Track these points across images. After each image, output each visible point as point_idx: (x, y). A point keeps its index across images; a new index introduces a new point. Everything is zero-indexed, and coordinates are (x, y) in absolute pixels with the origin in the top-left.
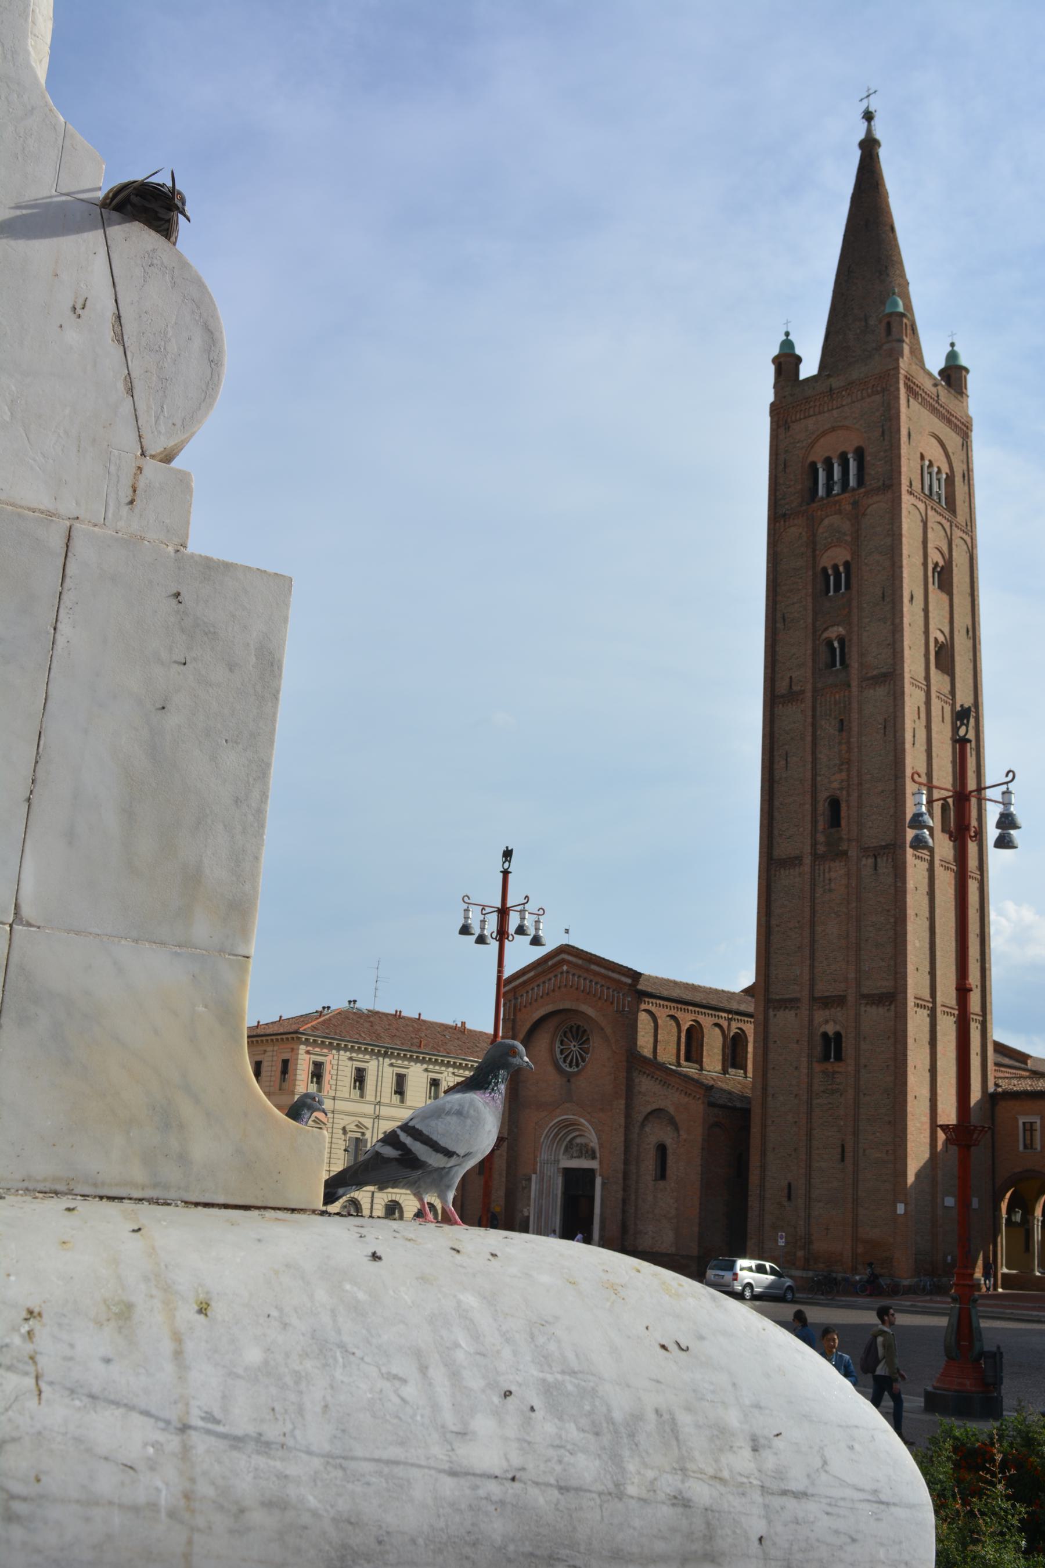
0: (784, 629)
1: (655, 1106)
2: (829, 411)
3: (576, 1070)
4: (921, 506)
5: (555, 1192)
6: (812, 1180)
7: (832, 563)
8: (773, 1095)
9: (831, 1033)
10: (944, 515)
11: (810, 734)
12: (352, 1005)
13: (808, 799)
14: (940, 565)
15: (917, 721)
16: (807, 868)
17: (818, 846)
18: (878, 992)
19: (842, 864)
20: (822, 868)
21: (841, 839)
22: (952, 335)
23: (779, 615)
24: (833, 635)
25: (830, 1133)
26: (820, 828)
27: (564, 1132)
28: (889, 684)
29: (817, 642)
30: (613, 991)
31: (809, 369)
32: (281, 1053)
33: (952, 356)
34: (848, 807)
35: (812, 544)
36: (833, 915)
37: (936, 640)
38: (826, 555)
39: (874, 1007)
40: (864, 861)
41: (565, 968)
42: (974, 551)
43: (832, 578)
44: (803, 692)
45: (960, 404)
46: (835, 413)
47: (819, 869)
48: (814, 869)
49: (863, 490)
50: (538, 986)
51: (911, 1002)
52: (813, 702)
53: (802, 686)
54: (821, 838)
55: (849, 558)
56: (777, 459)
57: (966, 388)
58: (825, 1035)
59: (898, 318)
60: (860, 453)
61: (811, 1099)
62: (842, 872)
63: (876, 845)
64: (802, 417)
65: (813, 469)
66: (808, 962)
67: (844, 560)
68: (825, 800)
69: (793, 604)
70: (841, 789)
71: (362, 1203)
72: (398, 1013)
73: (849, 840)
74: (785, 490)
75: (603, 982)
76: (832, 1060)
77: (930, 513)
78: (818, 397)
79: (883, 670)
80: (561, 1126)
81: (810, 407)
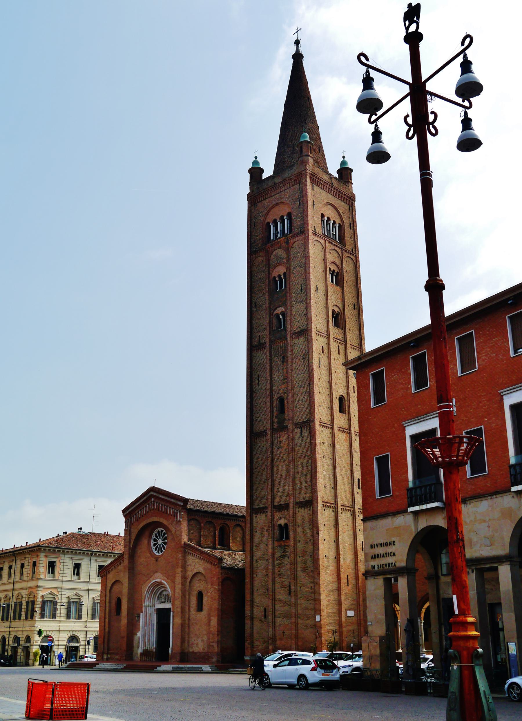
0: (256, 311)
1: (195, 571)
2: (274, 195)
3: (161, 554)
4: (322, 241)
5: (153, 622)
6: (276, 606)
7: (278, 274)
8: (256, 560)
9: (283, 525)
10: (337, 245)
11: (269, 365)
12: (80, 531)
13: (268, 399)
14: (336, 271)
15: (321, 353)
16: (269, 437)
17: (274, 424)
18: (304, 500)
19: (286, 433)
20: (276, 436)
21: (285, 419)
22: (344, 152)
23: (254, 304)
24: (279, 312)
25: (284, 579)
26: (275, 414)
27: (156, 589)
28: (306, 335)
29: (271, 316)
30: (175, 510)
32: (32, 558)
34: (287, 402)
35: (268, 264)
36: (282, 461)
37: (333, 311)
38: (275, 271)
39: (303, 508)
40: (296, 431)
41: (153, 499)
42: (358, 263)
43: (278, 282)
44: (265, 343)
45: (347, 188)
46: (277, 196)
47: (275, 437)
48: (272, 437)
49: (291, 235)
50: (141, 510)
52: (270, 348)
53: (265, 340)
54: (275, 420)
55: (285, 271)
56: (251, 222)
57: (351, 179)
58: (280, 525)
59: (306, 144)
60: (289, 215)
61: (274, 561)
62: (286, 437)
63: (301, 421)
64: (262, 199)
66: (270, 487)
67: (283, 272)
68: (277, 400)
69: (260, 297)
70: (284, 393)
71: (80, 637)
72: (106, 533)
73: (288, 420)
74: (255, 238)
75: (173, 507)
76: (284, 539)
77: (327, 244)
78: (269, 189)
79: (302, 328)
80: (154, 586)
81: (266, 194)
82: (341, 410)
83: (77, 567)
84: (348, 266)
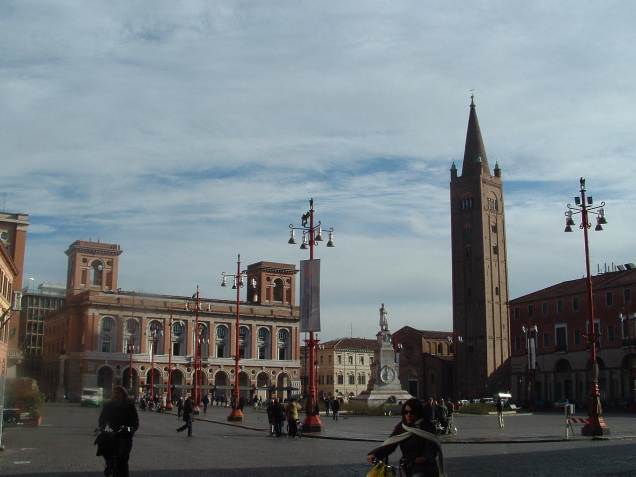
31: (459, 174)
33: (497, 165)
37: (493, 246)
51: (488, 338)
60: (472, 199)
65: (461, 201)
82: (497, 294)
83: (351, 358)
84: (500, 222)
